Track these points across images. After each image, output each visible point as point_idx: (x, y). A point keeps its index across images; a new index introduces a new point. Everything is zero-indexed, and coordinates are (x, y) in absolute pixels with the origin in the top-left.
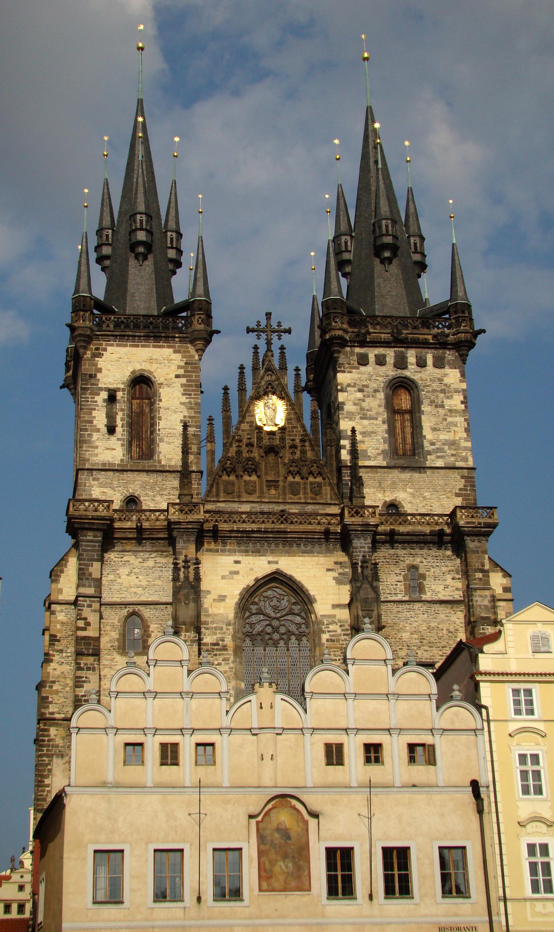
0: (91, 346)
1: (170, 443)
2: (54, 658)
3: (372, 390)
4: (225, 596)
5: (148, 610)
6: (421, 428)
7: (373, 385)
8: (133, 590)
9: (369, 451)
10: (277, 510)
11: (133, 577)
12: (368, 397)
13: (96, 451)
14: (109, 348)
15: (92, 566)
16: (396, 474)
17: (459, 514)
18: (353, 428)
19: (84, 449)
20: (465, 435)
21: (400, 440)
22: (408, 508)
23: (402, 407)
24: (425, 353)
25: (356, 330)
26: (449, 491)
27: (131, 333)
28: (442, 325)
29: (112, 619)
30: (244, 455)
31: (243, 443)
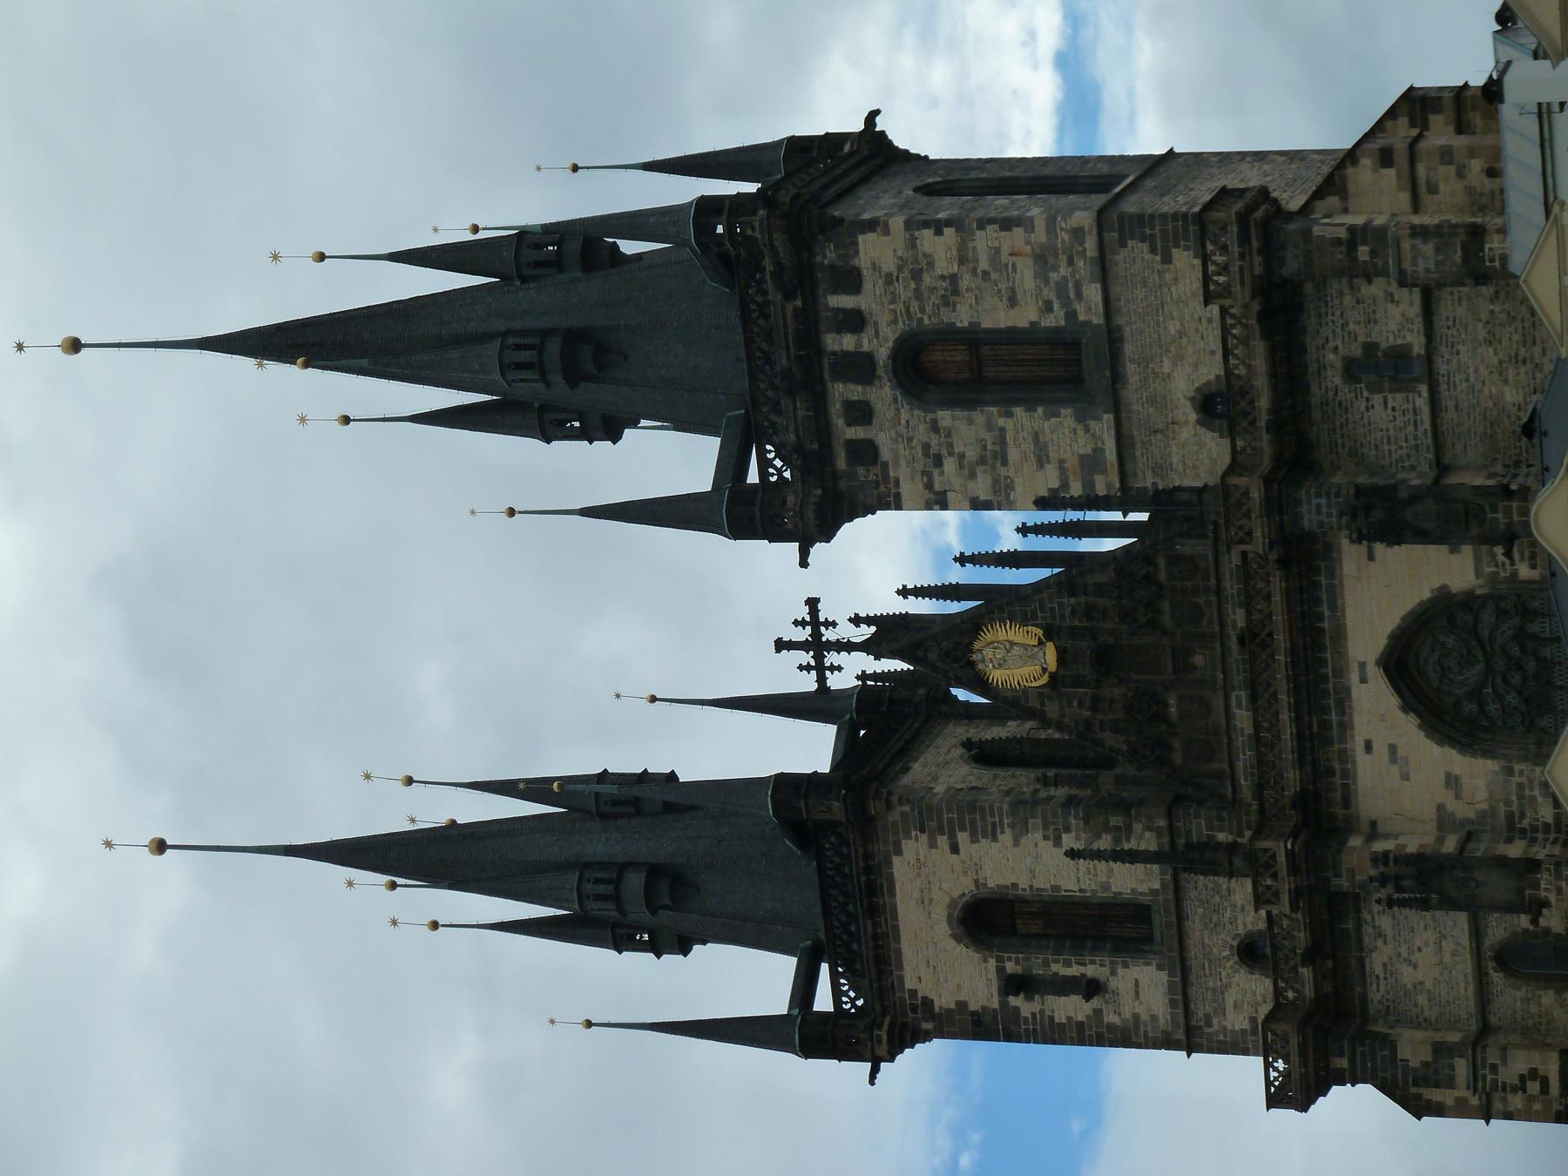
1: (1111, 871)
4: (1448, 775)
5: (1490, 932)
8: (1447, 958)
9: (1082, 451)
12: (950, 445)
13: (1144, 1017)
22: (1211, 370)
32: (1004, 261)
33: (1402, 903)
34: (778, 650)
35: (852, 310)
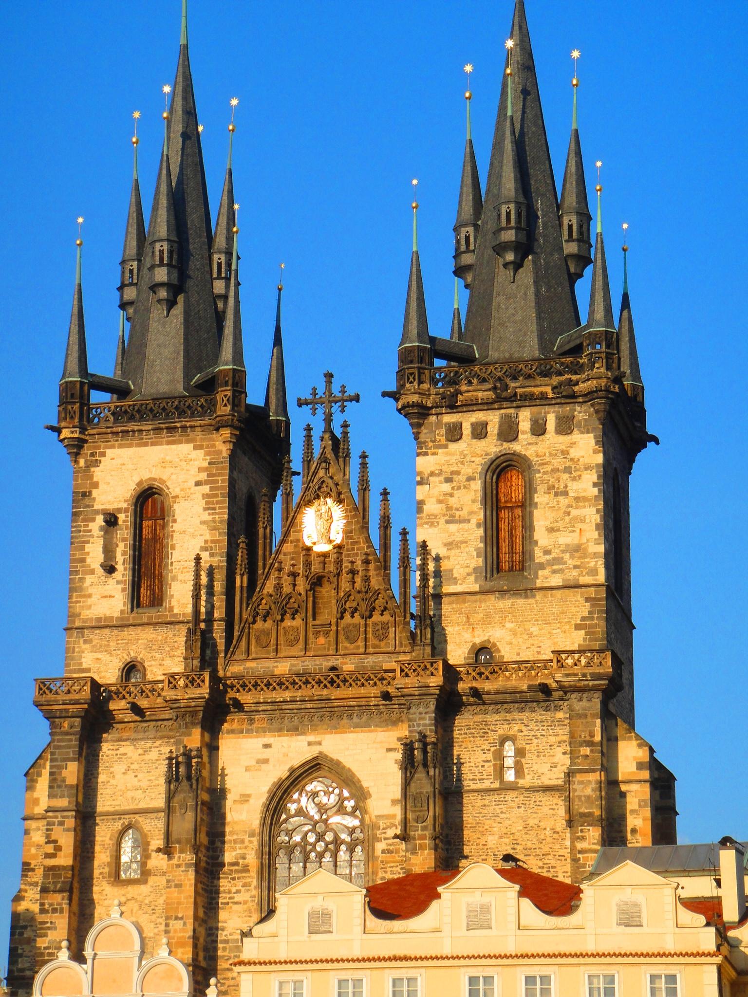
1: (185, 582)
2: (26, 895)
3: (465, 478)
4: (249, 796)
5: (148, 821)
7: (467, 470)
8: (129, 794)
9: (455, 571)
12: (459, 488)
13: (90, 601)
14: (108, 451)
16: (493, 603)
18: (424, 542)
19: (74, 600)
20: (595, 535)
21: (505, 547)
22: (507, 653)
25: (442, 390)
27: (136, 428)
33: (170, 766)
34: (326, 375)
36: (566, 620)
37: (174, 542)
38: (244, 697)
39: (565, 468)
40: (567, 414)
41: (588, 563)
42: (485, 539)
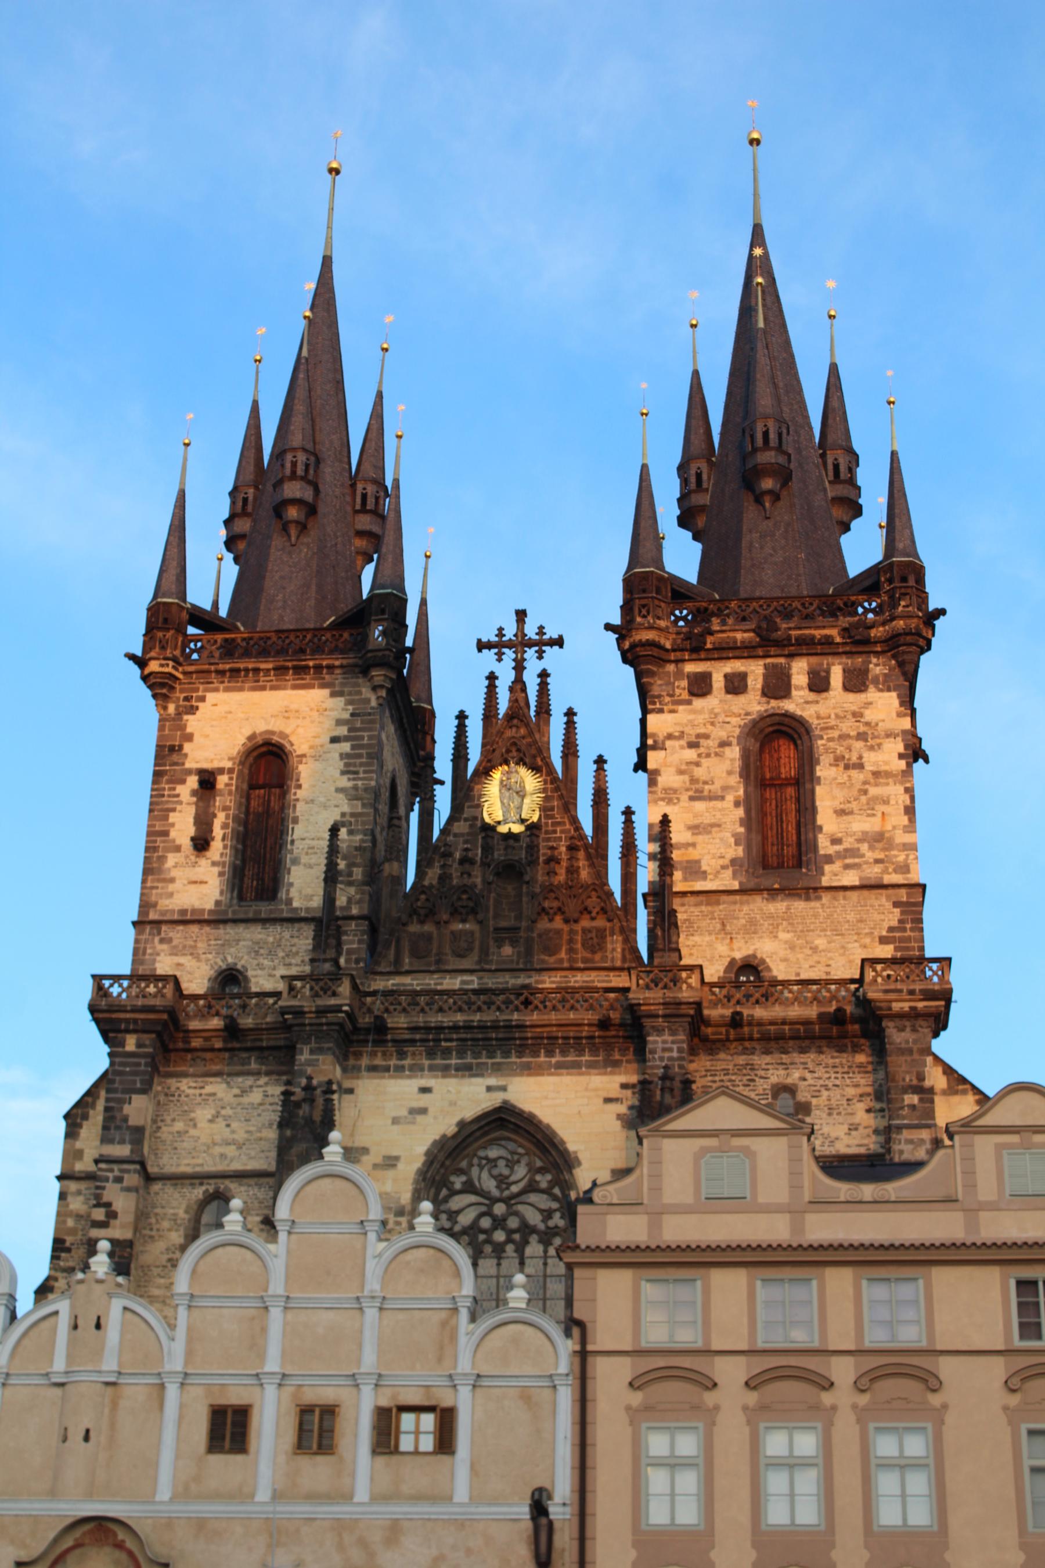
0: (178, 695)
1: (310, 867)
2: (56, 1284)
3: (717, 743)
4: (397, 1158)
5: (243, 1189)
6: (814, 810)
7: (719, 733)
8: (217, 1150)
10: (513, 985)
11: (221, 1123)
12: (708, 755)
13: (171, 887)
14: (210, 696)
15: (130, 1103)
16: (759, 906)
17: (870, 974)
18: (665, 816)
19: (149, 884)
22: (779, 971)
23: (780, 773)
24: (828, 664)
26: (866, 934)
27: (250, 666)
28: (863, 607)
29: (173, 1208)
30: (455, 882)
31: (454, 861)
32: (877, 807)
35: (829, 683)
36: (867, 931)
37: (298, 814)
38: (396, 1020)
39: (859, 734)
40: (859, 666)
41: (896, 856)
42: (747, 822)
